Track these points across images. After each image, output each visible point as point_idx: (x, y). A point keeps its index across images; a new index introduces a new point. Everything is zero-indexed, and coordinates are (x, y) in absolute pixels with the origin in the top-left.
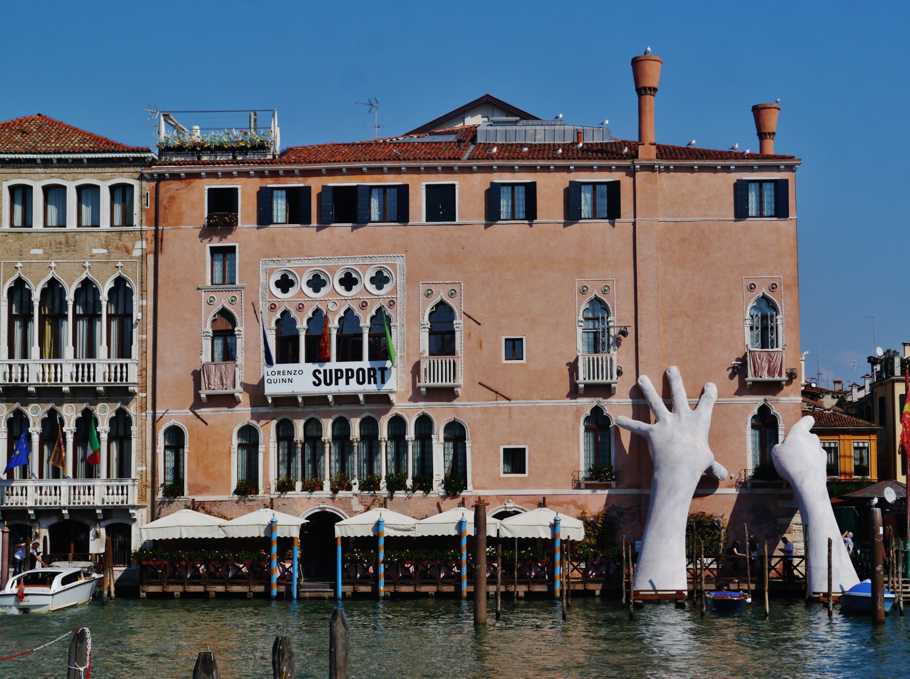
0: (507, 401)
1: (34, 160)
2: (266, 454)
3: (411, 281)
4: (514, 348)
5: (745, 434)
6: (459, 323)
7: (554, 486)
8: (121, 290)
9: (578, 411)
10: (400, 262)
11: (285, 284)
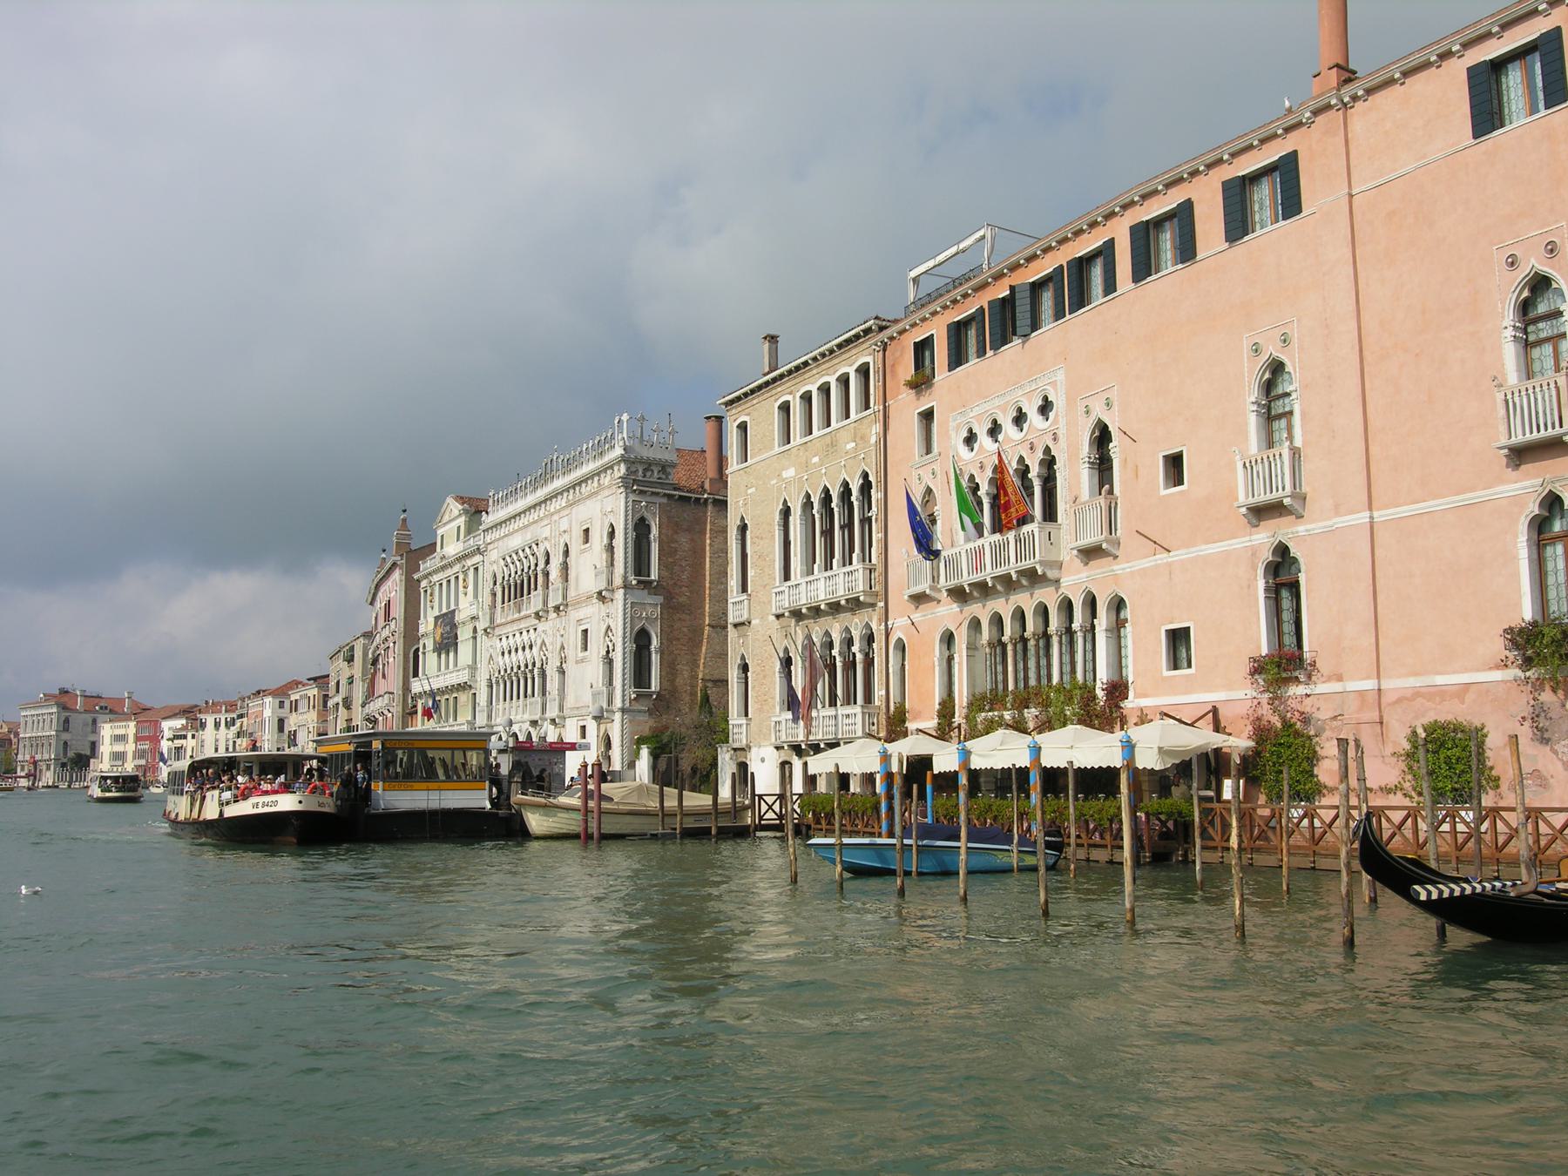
0: (1166, 554)
1: (806, 364)
2: (960, 664)
3: (1070, 401)
4: (1175, 465)
5: (1516, 558)
6: (1115, 448)
7: (1229, 687)
8: (866, 487)
9: (1254, 551)
10: (1060, 376)
11: (970, 439)
